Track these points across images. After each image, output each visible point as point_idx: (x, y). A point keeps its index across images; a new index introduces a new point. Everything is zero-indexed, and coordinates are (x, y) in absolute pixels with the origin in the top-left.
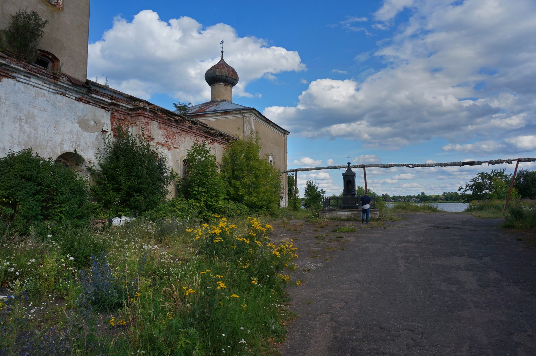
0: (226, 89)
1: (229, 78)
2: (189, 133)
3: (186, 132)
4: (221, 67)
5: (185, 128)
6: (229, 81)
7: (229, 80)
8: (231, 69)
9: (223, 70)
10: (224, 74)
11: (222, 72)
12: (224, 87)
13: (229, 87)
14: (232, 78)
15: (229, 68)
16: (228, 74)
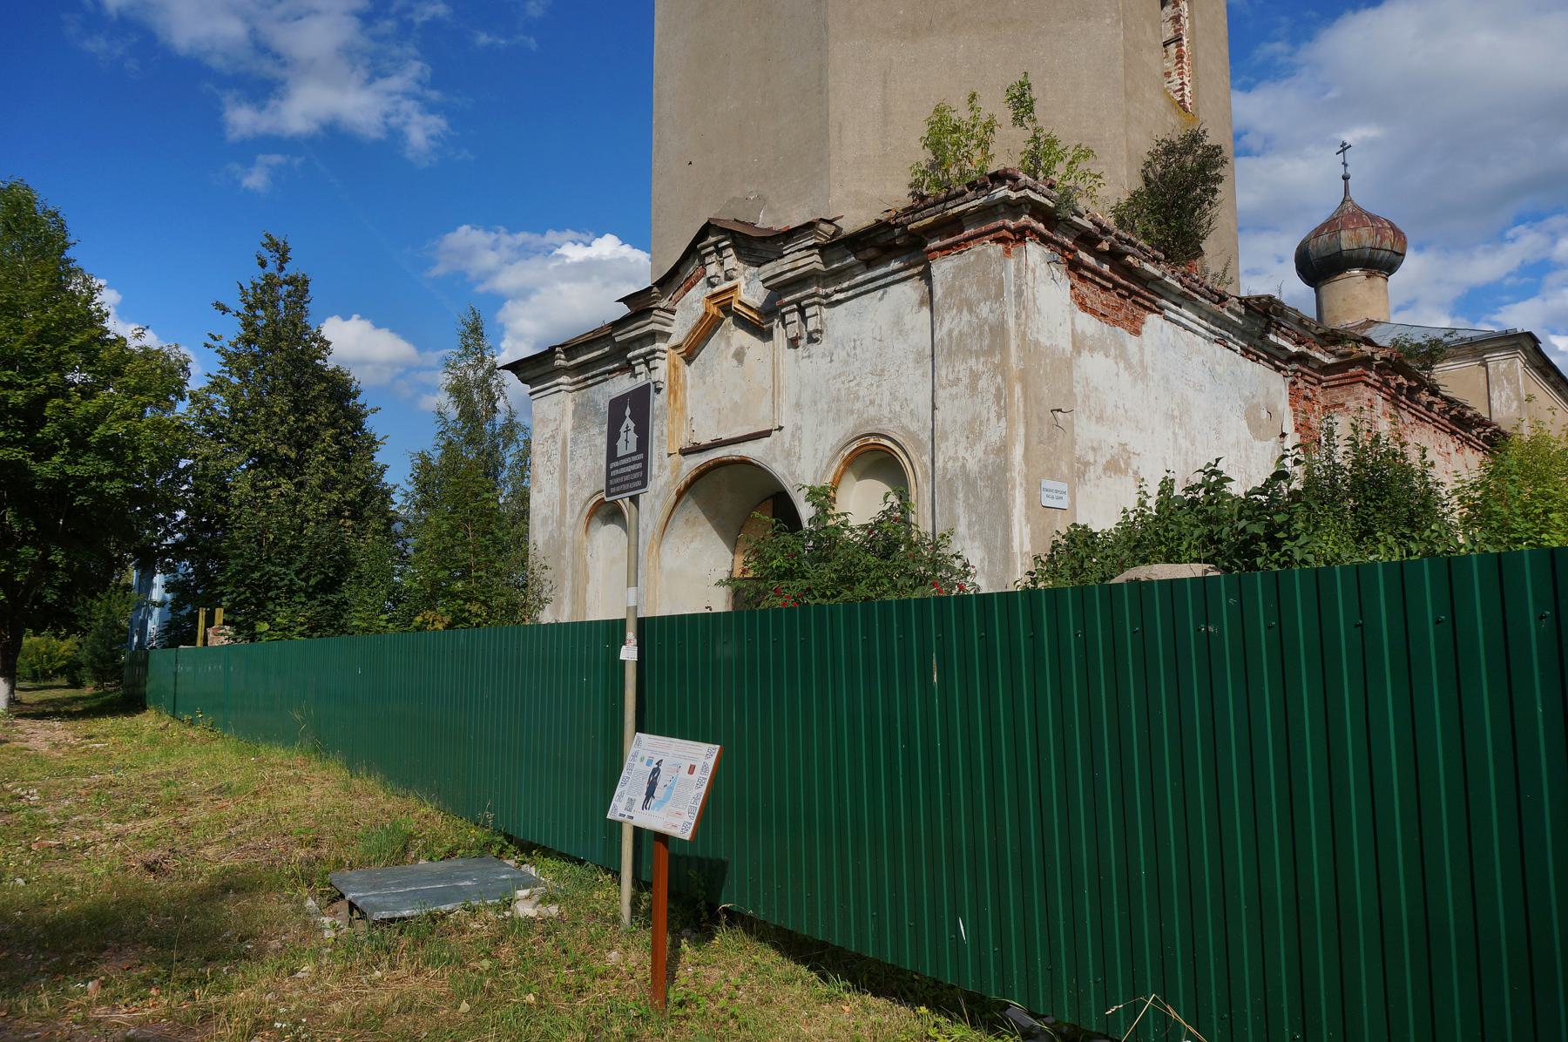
0: (1371, 288)
1: (1382, 253)
2: (1427, 425)
3: (1421, 419)
4: (1353, 223)
5: (1420, 408)
6: (1381, 261)
7: (1383, 257)
8: (1386, 224)
9: (1364, 232)
10: (1368, 244)
11: (1360, 237)
12: (1367, 283)
13: (1379, 281)
14: (1392, 251)
15: (1381, 222)
16: (1381, 242)
